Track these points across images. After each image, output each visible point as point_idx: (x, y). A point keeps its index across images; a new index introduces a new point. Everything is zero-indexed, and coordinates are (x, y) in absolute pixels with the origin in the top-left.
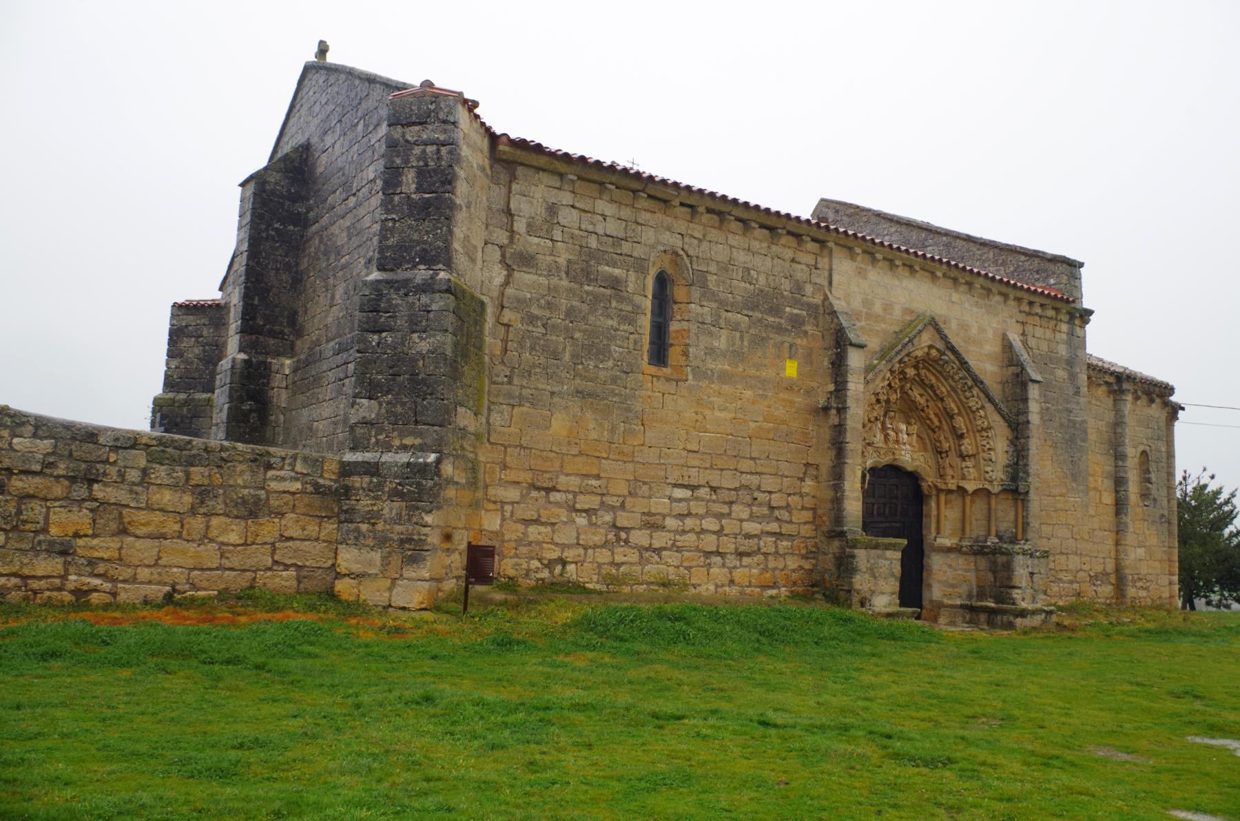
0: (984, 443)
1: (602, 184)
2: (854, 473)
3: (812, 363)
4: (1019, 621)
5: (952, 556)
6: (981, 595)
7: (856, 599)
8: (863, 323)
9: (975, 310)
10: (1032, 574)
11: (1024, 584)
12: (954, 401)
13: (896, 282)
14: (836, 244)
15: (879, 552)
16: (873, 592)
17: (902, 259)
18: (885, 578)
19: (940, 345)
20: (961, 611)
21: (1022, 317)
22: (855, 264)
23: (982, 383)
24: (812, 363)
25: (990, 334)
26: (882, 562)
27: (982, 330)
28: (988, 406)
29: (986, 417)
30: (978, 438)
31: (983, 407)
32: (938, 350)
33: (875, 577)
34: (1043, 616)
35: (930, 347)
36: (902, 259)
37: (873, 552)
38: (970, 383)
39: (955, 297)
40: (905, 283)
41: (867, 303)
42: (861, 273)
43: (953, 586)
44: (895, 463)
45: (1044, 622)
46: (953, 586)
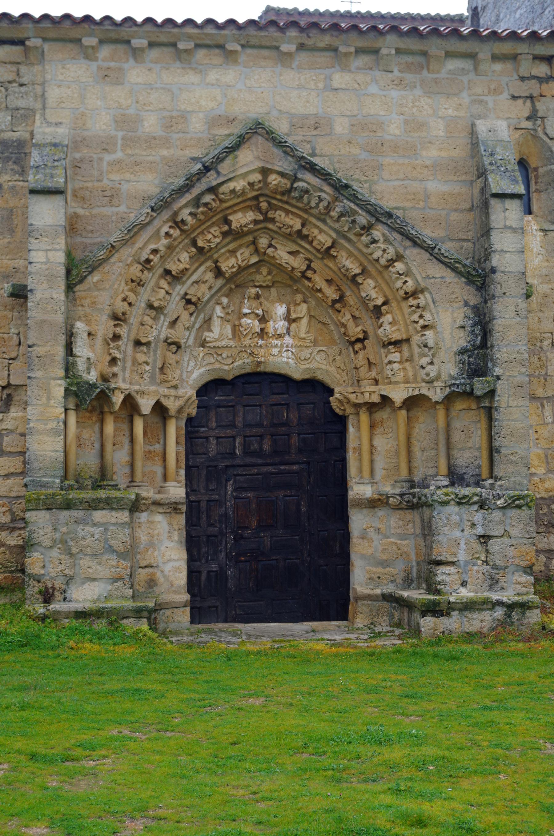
0: (415, 317)
1: (424, 54)
2: (48, 391)
3: (12, 231)
4: (428, 623)
5: (381, 512)
6: (408, 582)
7: (33, 589)
8: (119, 155)
9: (394, 94)
10: (484, 539)
11: (462, 556)
12: (350, 255)
13: (192, 78)
14: (45, 39)
15: (75, 513)
16: (69, 580)
17: (190, 37)
18: (94, 556)
19: (285, 165)
20: (386, 604)
21: (525, 89)
22: (94, 66)
23: (389, 215)
24: (12, 231)
25: (438, 129)
26: (80, 530)
27: (415, 125)
28: (413, 254)
29: (408, 273)
30: (407, 311)
31: (399, 257)
32: (282, 175)
33: (71, 555)
34: (499, 613)
35: (265, 172)
36: (190, 37)
37: (64, 515)
38: (363, 219)
39: (340, 79)
40: (213, 76)
41: (124, 121)
42: (106, 76)
43: (383, 564)
44: (261, 369)
45: (504, 623)
46: (383, 564)
